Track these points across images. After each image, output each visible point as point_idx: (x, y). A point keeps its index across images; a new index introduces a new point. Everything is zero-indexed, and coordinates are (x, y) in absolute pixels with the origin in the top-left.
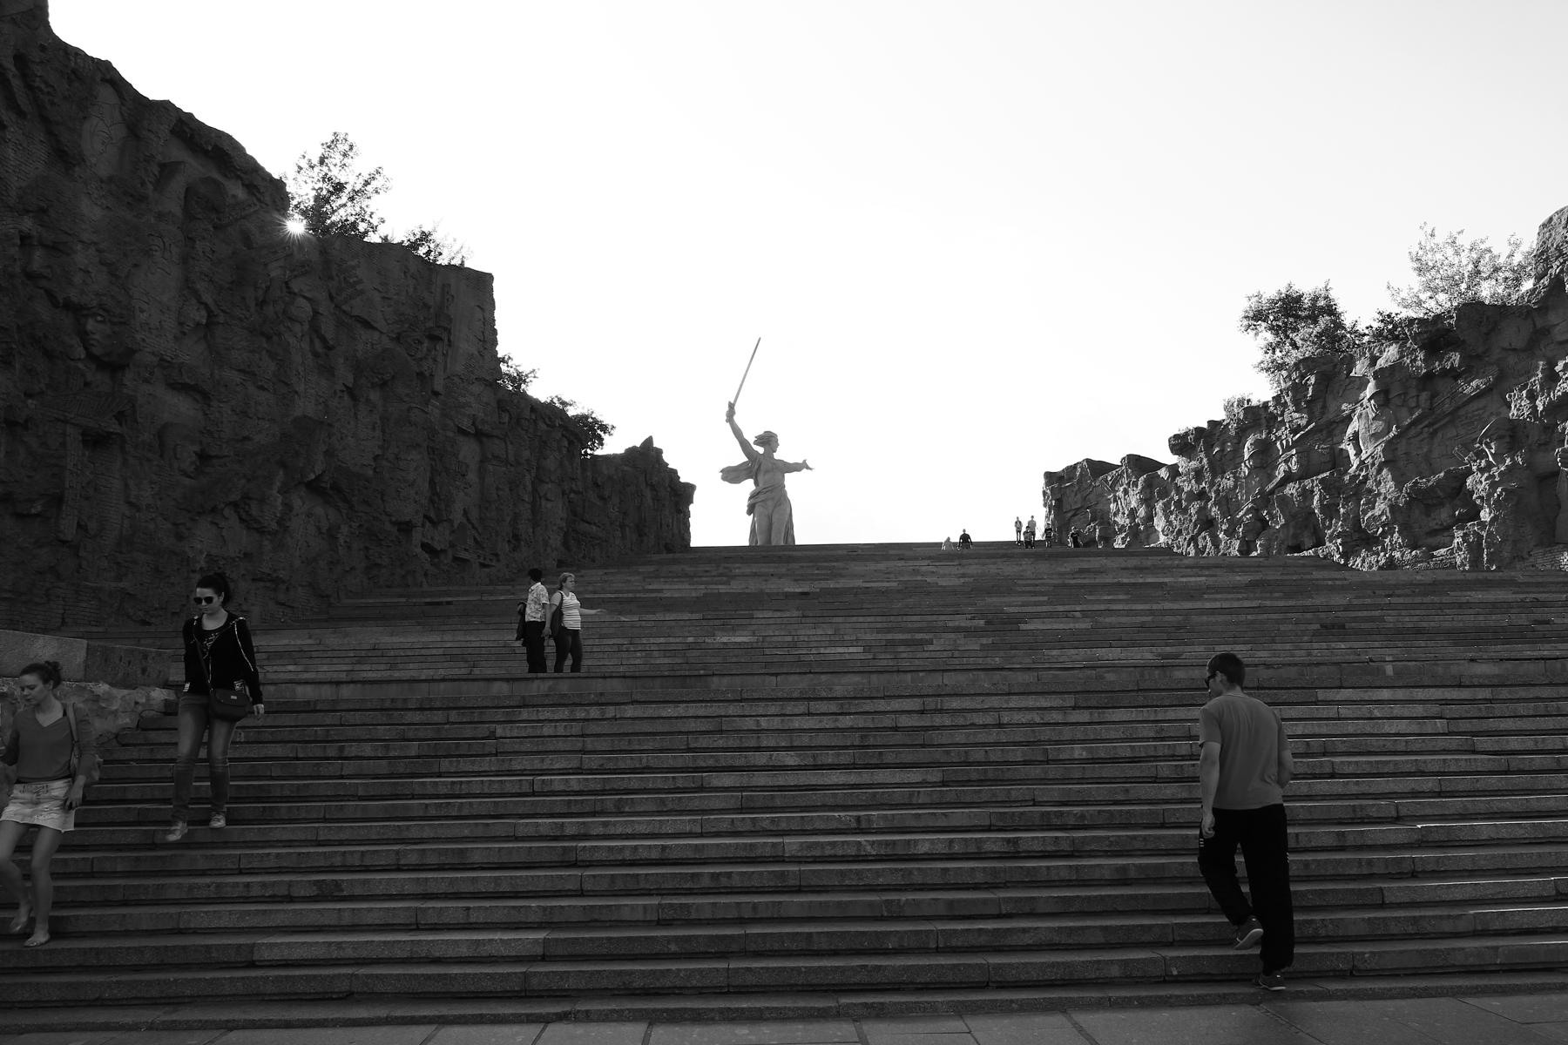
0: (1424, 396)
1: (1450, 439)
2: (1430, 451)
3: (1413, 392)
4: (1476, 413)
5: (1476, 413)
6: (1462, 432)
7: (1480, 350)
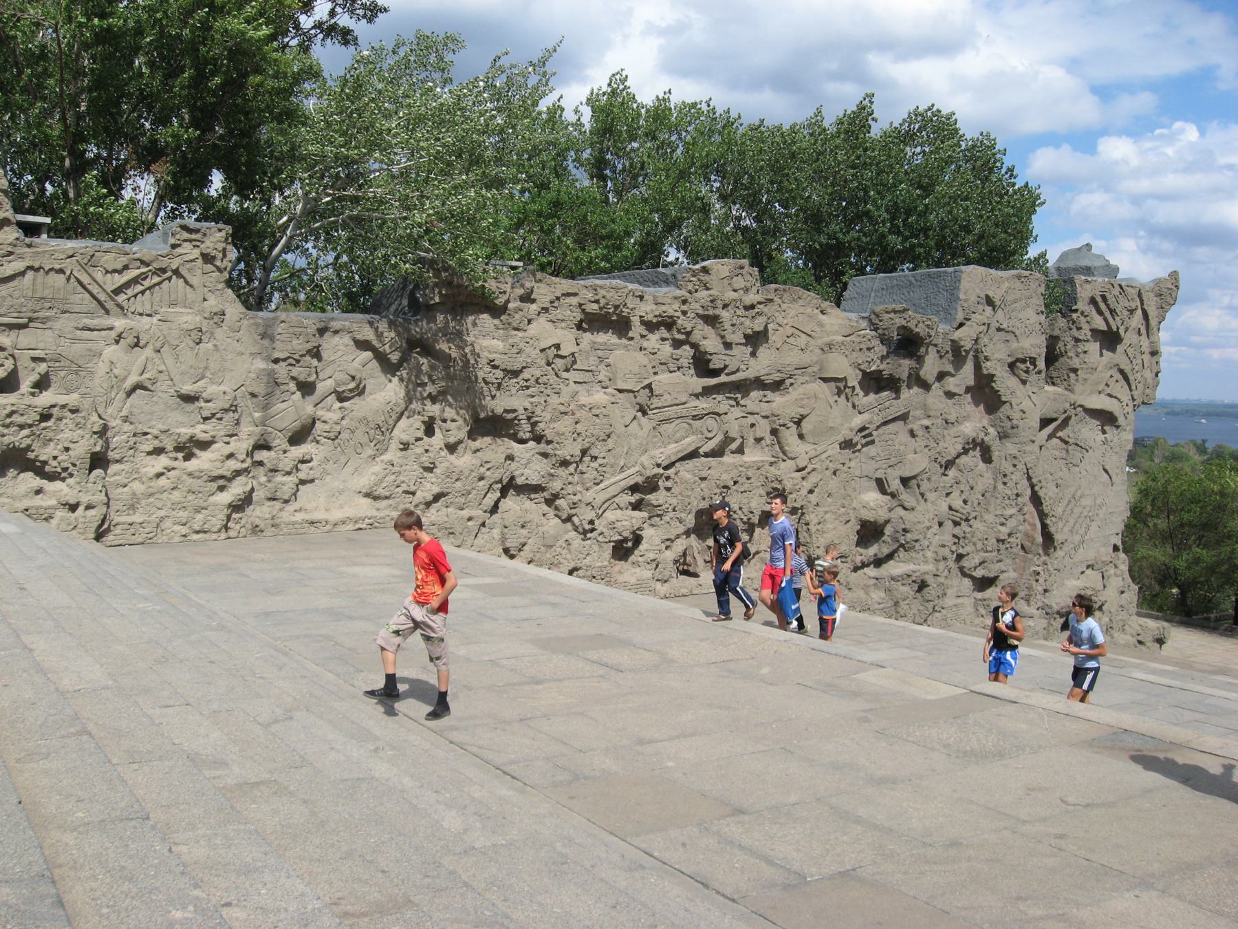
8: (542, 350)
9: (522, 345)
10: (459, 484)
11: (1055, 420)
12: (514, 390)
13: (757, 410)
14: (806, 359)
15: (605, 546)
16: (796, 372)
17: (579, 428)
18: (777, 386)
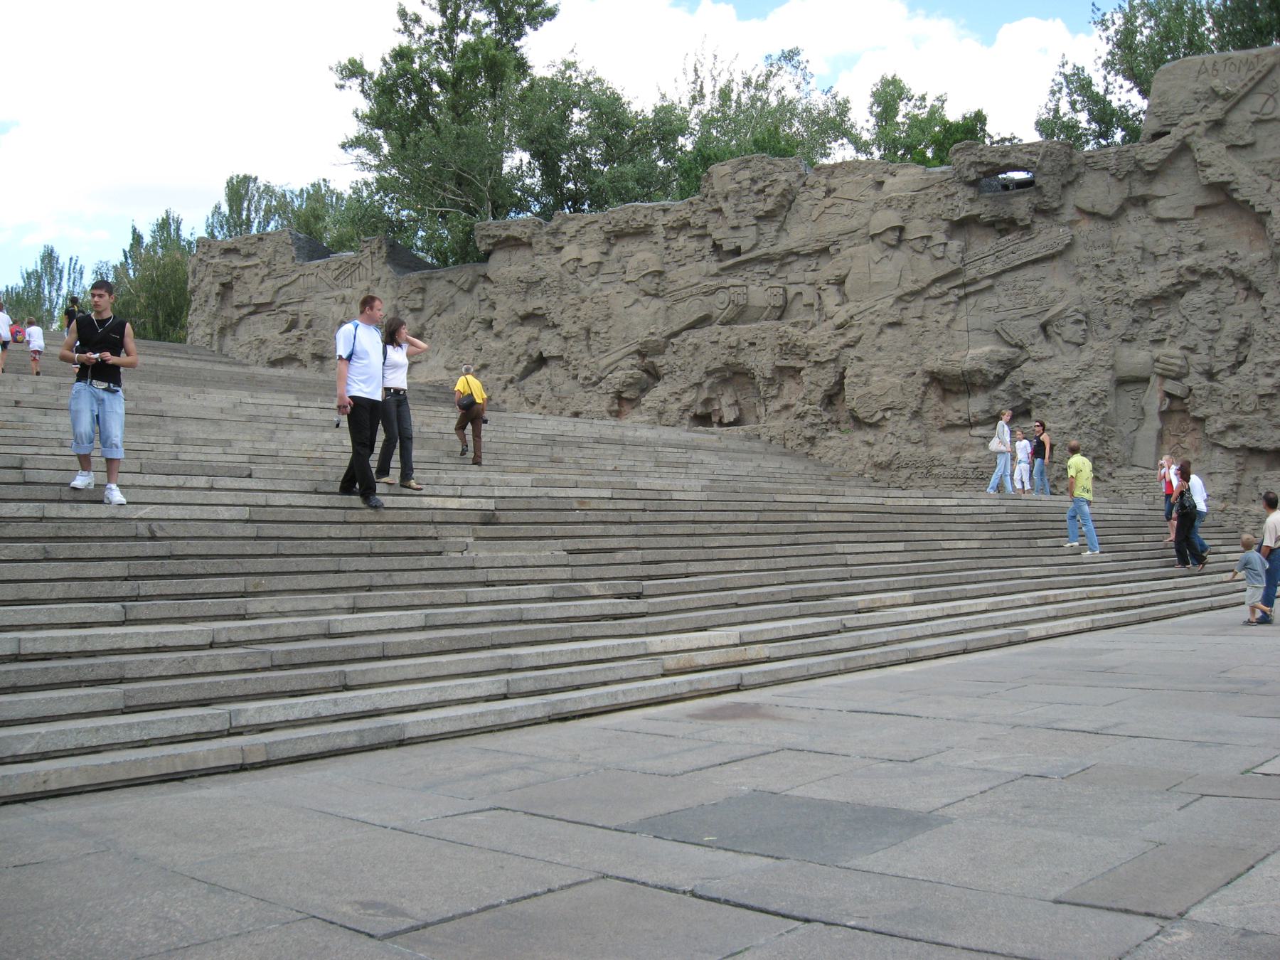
0: (955, 245)
1: (989, 309)
3: (940, 237)
4: (1029, 284)
5: (1029, 284)
7: (1055, 205)
8: (563, 265)
9: (541, 264)
10: (496, 358)
12: (540, 295)
13: (802, 280)
14: (853, 223)
15: (604, 397)
17: (579, 314)
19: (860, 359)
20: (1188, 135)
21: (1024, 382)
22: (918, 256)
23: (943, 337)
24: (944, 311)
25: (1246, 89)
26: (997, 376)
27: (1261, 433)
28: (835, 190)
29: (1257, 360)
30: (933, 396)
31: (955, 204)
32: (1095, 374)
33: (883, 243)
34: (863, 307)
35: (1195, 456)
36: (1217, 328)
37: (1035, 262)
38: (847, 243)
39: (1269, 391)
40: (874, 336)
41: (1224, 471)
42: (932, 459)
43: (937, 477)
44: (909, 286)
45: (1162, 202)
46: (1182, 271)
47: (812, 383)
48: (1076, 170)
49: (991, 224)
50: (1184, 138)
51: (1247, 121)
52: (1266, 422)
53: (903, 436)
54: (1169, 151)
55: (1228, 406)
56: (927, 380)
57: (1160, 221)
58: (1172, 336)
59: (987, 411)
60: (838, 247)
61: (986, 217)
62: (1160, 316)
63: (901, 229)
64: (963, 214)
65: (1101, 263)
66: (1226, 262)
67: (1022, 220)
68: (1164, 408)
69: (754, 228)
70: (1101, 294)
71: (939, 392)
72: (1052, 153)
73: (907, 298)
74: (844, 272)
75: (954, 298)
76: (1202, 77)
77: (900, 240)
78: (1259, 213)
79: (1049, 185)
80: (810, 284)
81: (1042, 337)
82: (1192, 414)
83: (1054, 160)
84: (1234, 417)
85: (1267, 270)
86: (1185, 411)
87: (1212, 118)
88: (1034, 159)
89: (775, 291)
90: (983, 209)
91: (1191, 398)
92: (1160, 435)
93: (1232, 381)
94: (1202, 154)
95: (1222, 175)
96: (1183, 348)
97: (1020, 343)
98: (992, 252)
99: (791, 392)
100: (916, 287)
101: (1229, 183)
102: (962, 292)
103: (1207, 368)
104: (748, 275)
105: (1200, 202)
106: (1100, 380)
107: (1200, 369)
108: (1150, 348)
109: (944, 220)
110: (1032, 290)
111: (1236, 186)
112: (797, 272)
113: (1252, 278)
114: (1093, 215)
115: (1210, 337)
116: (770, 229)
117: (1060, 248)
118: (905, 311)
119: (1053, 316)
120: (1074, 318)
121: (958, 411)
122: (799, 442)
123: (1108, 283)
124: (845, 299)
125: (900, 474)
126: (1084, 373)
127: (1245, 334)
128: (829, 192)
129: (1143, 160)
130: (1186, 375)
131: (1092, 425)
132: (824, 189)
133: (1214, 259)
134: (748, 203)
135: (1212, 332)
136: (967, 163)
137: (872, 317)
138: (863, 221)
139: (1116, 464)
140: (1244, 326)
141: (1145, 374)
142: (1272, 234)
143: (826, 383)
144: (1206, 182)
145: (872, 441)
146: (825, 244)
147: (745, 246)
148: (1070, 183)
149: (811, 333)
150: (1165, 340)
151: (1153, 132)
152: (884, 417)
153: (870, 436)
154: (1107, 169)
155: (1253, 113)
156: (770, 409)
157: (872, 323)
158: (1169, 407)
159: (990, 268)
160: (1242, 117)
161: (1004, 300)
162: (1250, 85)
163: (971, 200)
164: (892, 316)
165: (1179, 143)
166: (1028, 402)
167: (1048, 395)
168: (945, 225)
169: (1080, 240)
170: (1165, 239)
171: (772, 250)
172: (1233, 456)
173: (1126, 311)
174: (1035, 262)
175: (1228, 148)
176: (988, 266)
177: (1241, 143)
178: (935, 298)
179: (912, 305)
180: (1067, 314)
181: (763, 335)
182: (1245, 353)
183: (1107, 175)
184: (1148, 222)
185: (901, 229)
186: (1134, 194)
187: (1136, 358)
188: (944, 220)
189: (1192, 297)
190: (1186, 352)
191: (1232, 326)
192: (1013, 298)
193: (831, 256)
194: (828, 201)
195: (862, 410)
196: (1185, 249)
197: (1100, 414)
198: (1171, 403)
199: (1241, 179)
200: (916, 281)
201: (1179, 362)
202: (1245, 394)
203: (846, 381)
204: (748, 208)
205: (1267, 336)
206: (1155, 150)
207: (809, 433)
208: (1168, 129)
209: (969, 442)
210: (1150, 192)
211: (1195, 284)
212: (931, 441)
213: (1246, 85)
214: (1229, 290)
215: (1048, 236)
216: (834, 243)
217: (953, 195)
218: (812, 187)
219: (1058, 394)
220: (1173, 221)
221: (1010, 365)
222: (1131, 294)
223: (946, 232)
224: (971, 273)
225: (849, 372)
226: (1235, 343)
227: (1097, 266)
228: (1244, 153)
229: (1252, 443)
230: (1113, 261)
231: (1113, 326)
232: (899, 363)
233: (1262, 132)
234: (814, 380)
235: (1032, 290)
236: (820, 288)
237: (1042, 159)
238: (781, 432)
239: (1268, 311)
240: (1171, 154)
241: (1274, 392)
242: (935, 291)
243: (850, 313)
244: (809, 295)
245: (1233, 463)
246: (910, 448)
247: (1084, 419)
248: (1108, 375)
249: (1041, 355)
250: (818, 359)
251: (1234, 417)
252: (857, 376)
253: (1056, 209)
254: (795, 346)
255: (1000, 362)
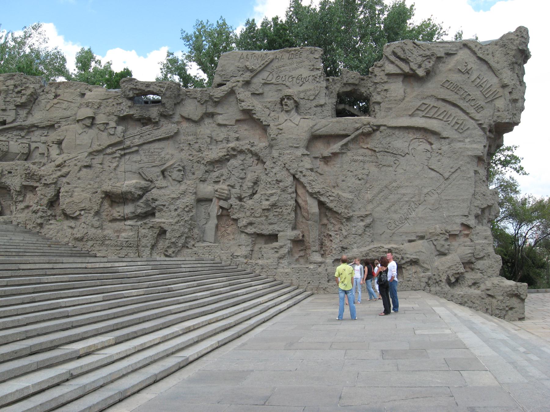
0: (120, 128)
1: (136, 162)
2: (117, 166)
3: (112, 124)
6: (146, 160)
7: (171, 113)
11: (347, 136)
13: (39, 140)
14: (68, 113)
16: (60, 120)
18: (51, 127)
19: (68, 184)
20: (234, 86)
21: (152, 199)
22: (101, 133)
23: (112, 174)
24: (113, 161)
25: (261, 68)
26: (139, 195)
27: (263, 227)
28: (59, 95)
29: (262, 193)
30: (106, 204)
31: (121, 108)
32: (187, 196)
33: (84, 124)
34: (71, 156)
35: (233, 237)
36: (244, 177)
37: (159, 140)
38: (64, 123)
39: (267, 207)
40: (76, 172)
41: (246, 244)
42: (105, 236)
43: (107, 245)
44: (95, 147)
45: (221, 116)
46: (229, 149)
47: (42, 195)
48: (181, 97)
49: (139, 120)
50: (233, 87)
51: (260, 83)
52: (265, 222)
53: (90, 224)
54: (226, 92)
55: (248, 214)
56: (103, 196)
57: (219, 125)
58: (224, 180)
59: (134, 213)
60: (59, 125)
61: (137, 116)
62: (218, 170)
63: (93, 118)
64: (125, 114)
65: (191, 143)
66: (249, 147)
67: (154, 119)
68: (219, 214)
69: (14, 111)
70: (191, 158)
71: (109, 202)
72: (171, 88)
73: (95, 153)
74: (62, 138)
75: (118, 155)
76: (241, 60)
77: (92, 124)
78: (265, 125)
79: (169, 103)
80: (43, 143)
81: (161, 177)
82: (232, 217)
83: (171, 91)
84: (251, 219)
85: (267, 151)
86: (228, 216)
87: (245, 80)
88: (162, 89)
89: (24, 145)
90: (135, 112)
91: (232, 209)
92: (217, 227)
93: (250, 202)
94: (240, 95)
95: (249, 106)
96: (229, 185)
97: (151, 179)
98: (139, 133)
99: (31, 199)
100: (99, 148)
101: (252, 110)
102: (123, 153)
103: (239, 195)
104: (10, 135)
105: (238, 118)
106: (189, 199)
107: (236, 196)
108: (213, 185)
109: (115, 116)
110: (157, 154)
111: (255, 112)
112: (36, 136)
113: (260, 155)
114: (188, 120)
115: (241, 181)
116: (23, 113)
117: (172, 134)
118: (93, 160)
119: (168, 167)
120: (178, 168)
121: (119, 212)
122: (34, 226)
123: (195, 153)
124: (61, 152)
125: (88, 244)
126: (182, 195)
127: (256, 180)
128: (56, 96)
129: (213, 96)
130: (230, 198)
131: (186, 221)
132: (54, 94)
133: (244, 145)
134: (12, 97)
135: (242, 179)
136: (129, 88)
137: (76, 162)
138: (74, 112)
139: (196, 241)
140: (256, 177)
141: (211, 197)
142: (270, 135)
143: (50, 195)
144: (241, 109)
145: (73, 226)
146: (53, 123)
147: (9, 120)
148: (178, 103)
149: (43, 168)
150: (220, 181)
151: (219, 83)
152: (80, 214)
153: (72, 223)
154: (196, 98)
155: (263, 79)
156: (18, 208)
157: (76, 165)
158: (221, 213)
159: (137, 141)
160: (258, 81)
161: (144, 158)
162: (263, 67)
163: (130, 107)
164: (87, 162)
165: (230, 89)
166: (154, 209)
167: (164, 206)
168: (116, 118)
169: (182, 131)
170: (222, 134)
171: (23, 123)
172: (250, 237)
173: (202, 167)
174: (159, 140)
175: (251, 94)
176: (137, 140)
177: (257, 92)
178: (109, 154)
179: (97, 157)
180: (174, 166)
181: (16, 168)
182: (256, 189)
183: (196, 101)
184: (214, 125)
185: (93, 118)
186: (208, 111)
187: (207, 189)
188: (115, 116)
189: (233, 162)
190: (230, 187)
191: (251, 176)
192: (148, 157)
193: (55, 129)
194: (56, 101)
195: (68, 210)
196: (230, 139)
197: (190, 215)
198: (222, 211)
199: (257, 109)
200: (100, 145)
201: (226, 192)
202: (256, 209)
203: (61, 194)
204: (12, 100)
205: (266, 182)
206: (219, 91)
207: (39, 221)
208: (225, 82)
209: (124, 228)
210: (215, 111)
211: (235, 156)
212: (104, 227)
213: (261, 66)
214: (250, 160)
215: (167, 128)
216: (58, 123)
217: (120, 104)
218: (47, 93)
219: (169, 205)
220: (225, 125)
221: (146, 190)
222: (205, 159)
223: (116, 122)
224: (128, 143)
225: (62, 190)
226: (252, 184)
227: (190, 144)
228: (258, 97)
229: (259, 232)
230: (197, 142)
231: (196, 173)
232: (89, 186)
233: (267, 88)
234: (43, 193)
235: (157, 154)
236: (48, 145)
237: (166, 90)
238: (24, 220)
239: (268, 170)
240: (226, 94)
241: (270, 208)
242: (109, 151)
243: (64, 159)
244: (42, 149)
245: (250, 240)
246: (93, 230)
247: (182, 218)
248: (193, 197)
249: (161, 186)
250: (46, 182)
251: (251, 219)
252: (66, 192)
253: (171, 115)
254: (33, 175)
255: (141, 188)
